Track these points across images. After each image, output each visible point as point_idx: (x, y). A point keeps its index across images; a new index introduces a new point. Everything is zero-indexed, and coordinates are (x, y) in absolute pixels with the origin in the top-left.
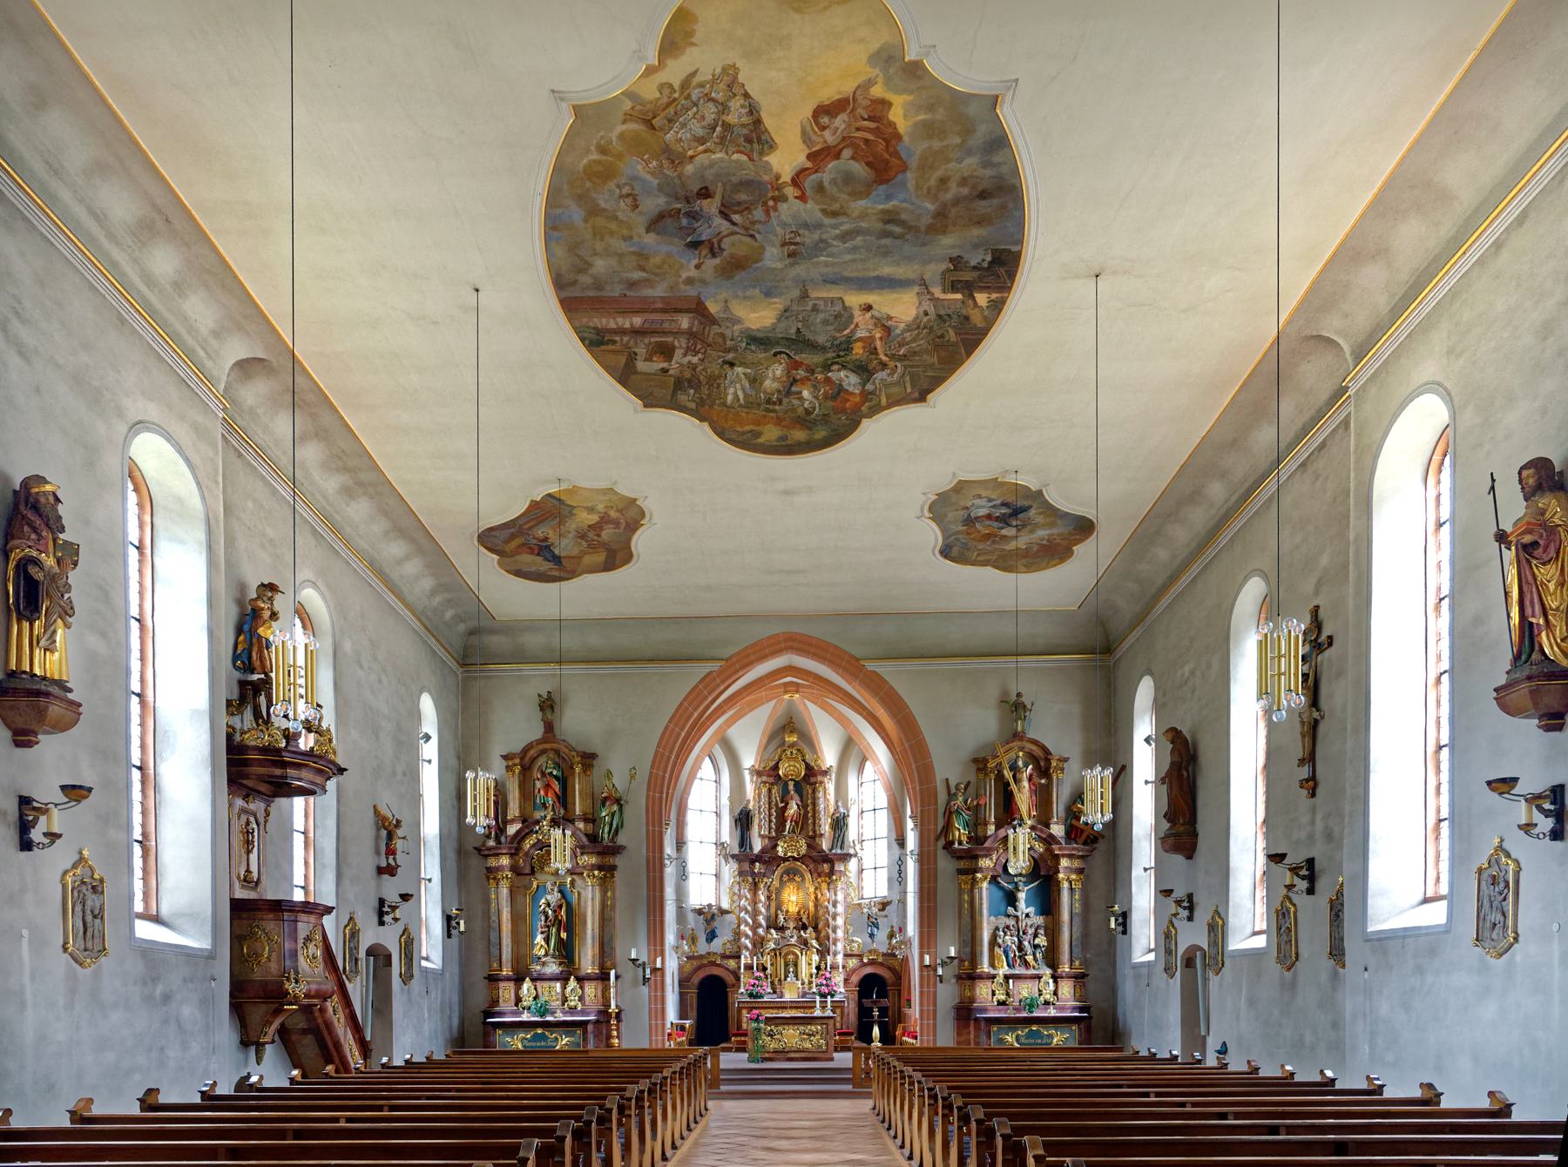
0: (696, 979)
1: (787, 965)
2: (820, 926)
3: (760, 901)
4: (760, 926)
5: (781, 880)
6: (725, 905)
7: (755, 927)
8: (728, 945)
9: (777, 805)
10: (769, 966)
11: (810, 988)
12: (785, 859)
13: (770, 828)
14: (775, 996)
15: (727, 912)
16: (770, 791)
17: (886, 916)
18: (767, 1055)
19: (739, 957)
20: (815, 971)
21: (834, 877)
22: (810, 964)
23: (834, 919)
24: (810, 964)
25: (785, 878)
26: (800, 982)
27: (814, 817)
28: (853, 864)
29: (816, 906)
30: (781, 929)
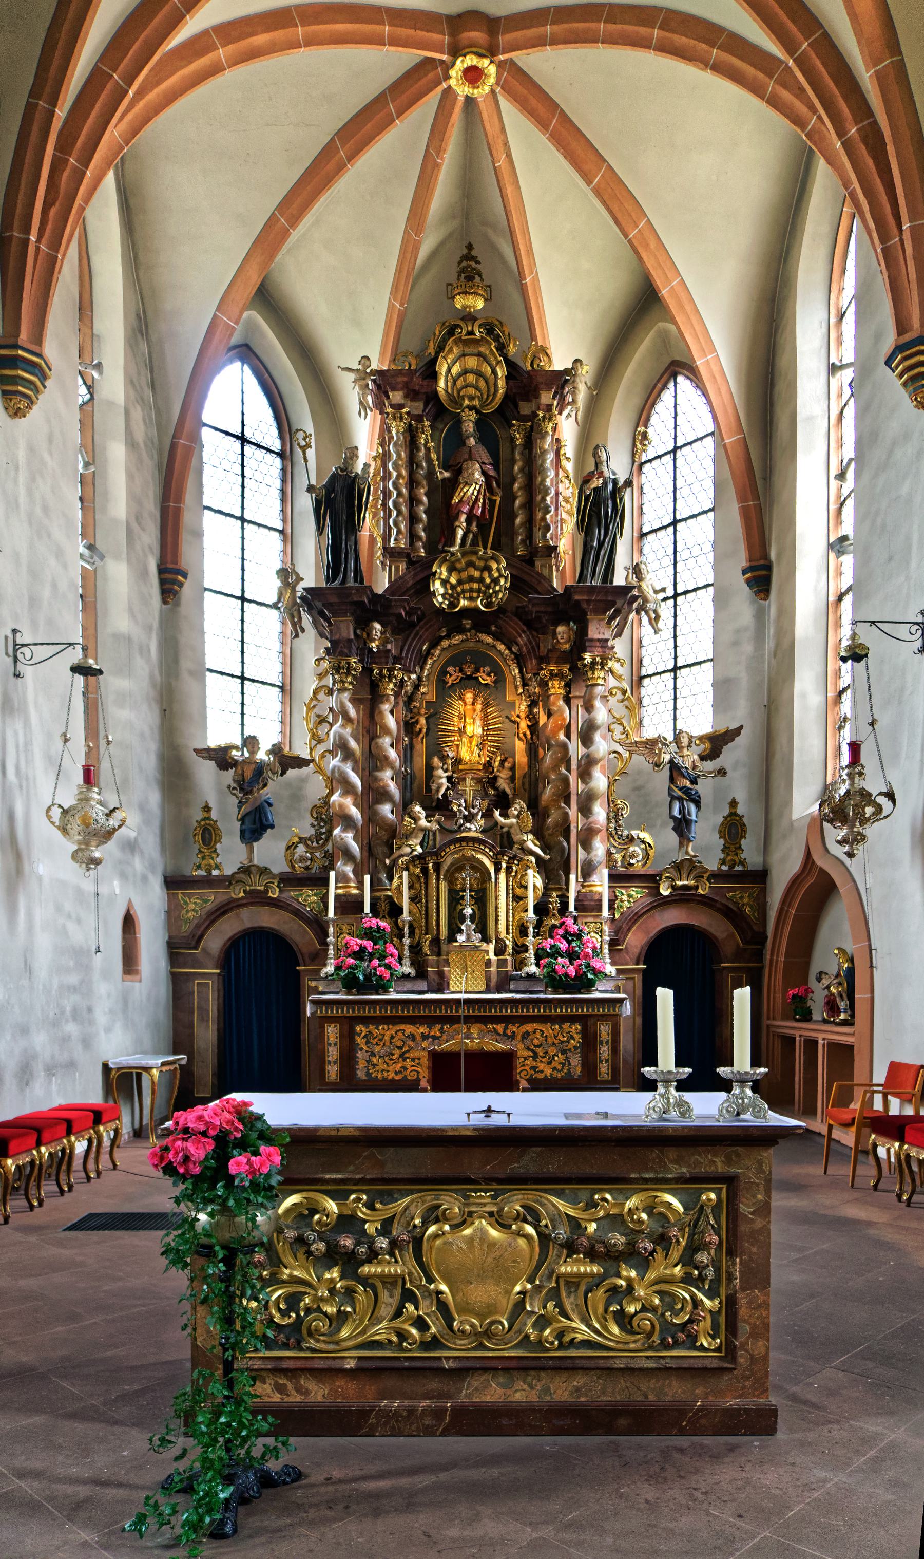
1: (455, 899)
2: (548, 792)
3: (386, 731)
8: (301, 849)
11: (520, 964)
14: (423, 985)
16: (411, 435)
17: (722, 772)
19: (325, 882)
20: (531, 914)
21: (588, 658)
23: (585, 774)
24: (518, 898)
26: (491, 947)
27: (530, 506)
29: (532, 751)
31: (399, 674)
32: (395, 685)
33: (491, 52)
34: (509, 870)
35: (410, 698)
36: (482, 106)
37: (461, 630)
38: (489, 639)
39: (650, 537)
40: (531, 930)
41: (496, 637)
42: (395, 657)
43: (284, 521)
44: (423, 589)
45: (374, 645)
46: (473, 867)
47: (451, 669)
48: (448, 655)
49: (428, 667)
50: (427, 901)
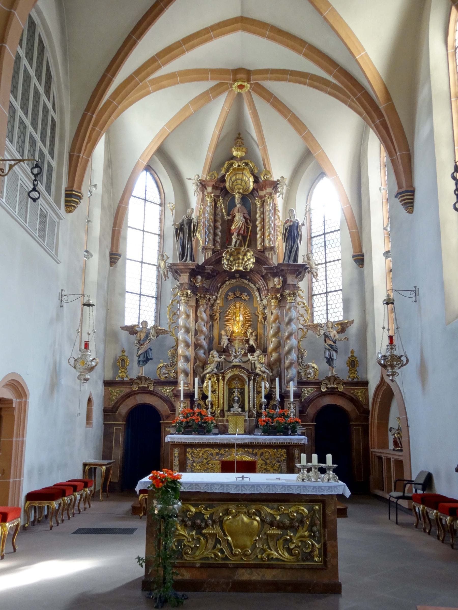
0: (124, 410)
4: (201, 347)
5: (226, 299)
6: (165, 326)
7: (197, 346)
9: (223, 216)
10: (209, 394)
12: (232, 276)
13: (215, 242)
15: (164, 332)
18: (186, 575)
20: (264, 400)
22: (259, 392)
25: (231, 296)
26: (247, 414)
28: (302, 285)
30: (224, 351)
31: (208, 296)
32: (207, 300)
33: (248, 80)
34: (254, 380)
35: (213, 305)
36: (243, 95)
37: (234, 277)
38: (246, 281)
39: (315, 239)
40: (264, 407)
41: (250, 280)
42: (207, 289)
43: (161, 230)
44: (219, 261)
45: (198, 285)
46: (239, 379)
47: (230, 294)
48: (229, 287)
49: (220, 292)
50: (219, 393)
